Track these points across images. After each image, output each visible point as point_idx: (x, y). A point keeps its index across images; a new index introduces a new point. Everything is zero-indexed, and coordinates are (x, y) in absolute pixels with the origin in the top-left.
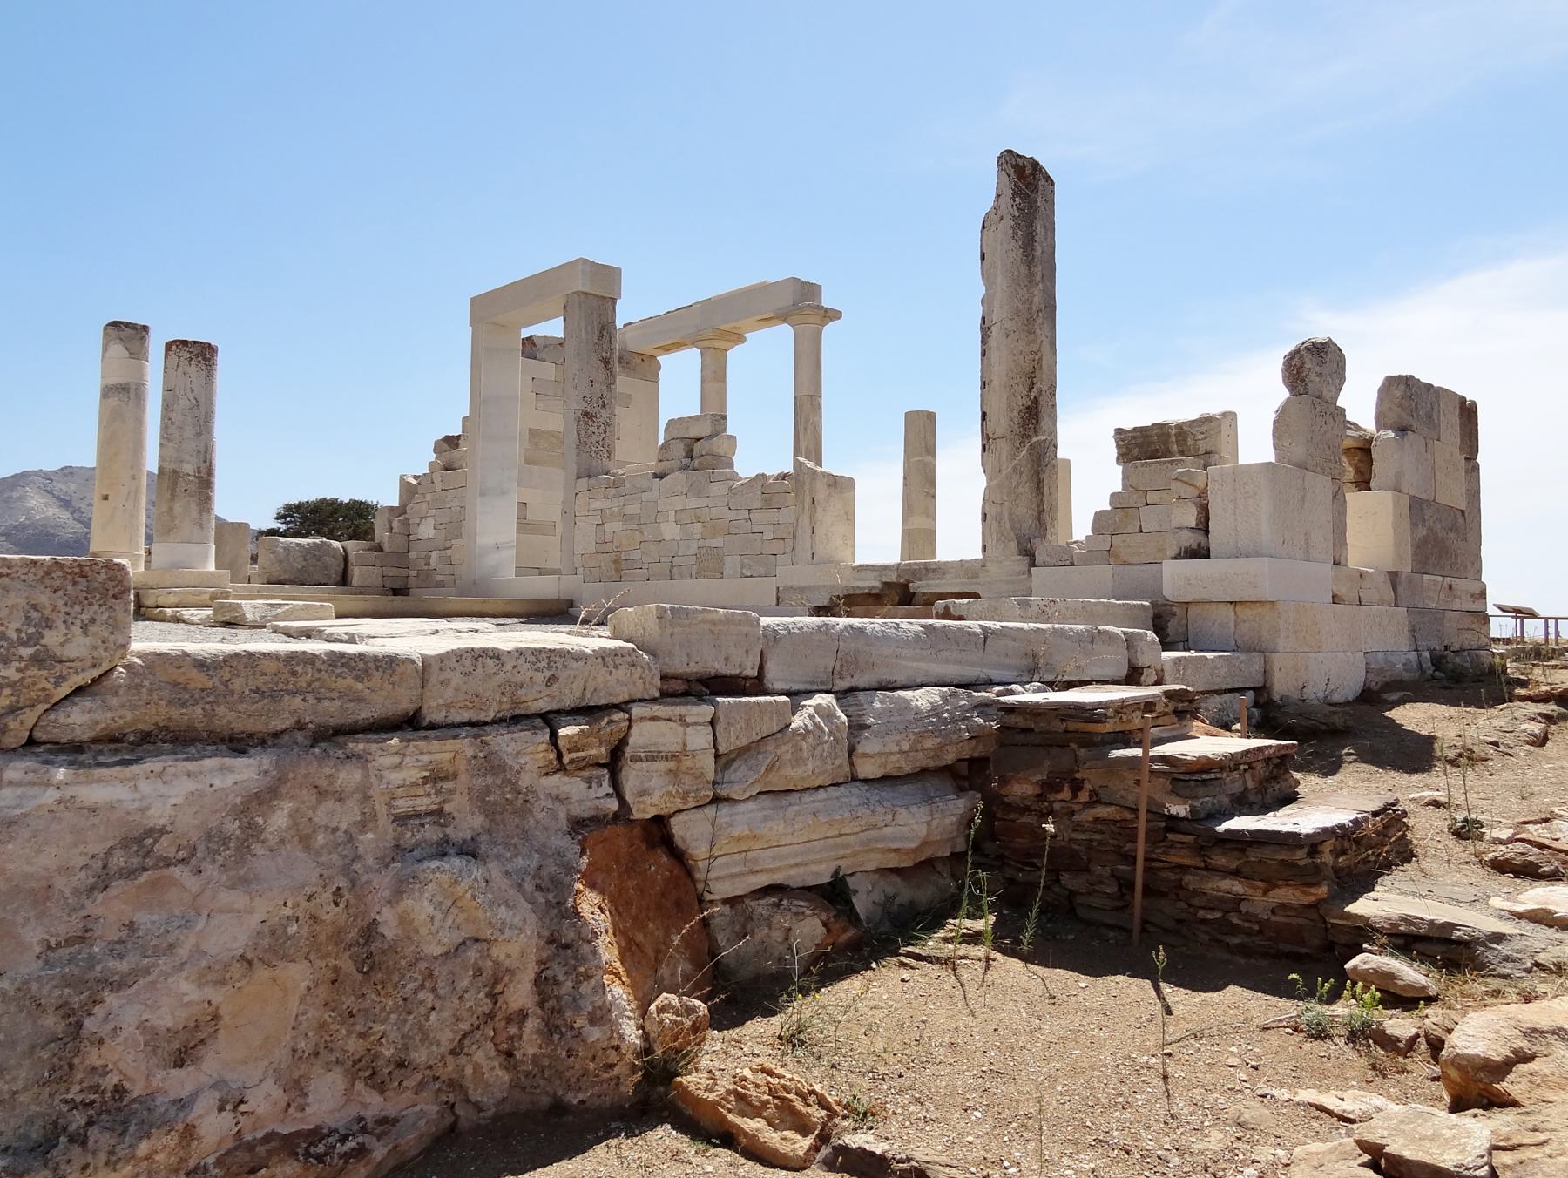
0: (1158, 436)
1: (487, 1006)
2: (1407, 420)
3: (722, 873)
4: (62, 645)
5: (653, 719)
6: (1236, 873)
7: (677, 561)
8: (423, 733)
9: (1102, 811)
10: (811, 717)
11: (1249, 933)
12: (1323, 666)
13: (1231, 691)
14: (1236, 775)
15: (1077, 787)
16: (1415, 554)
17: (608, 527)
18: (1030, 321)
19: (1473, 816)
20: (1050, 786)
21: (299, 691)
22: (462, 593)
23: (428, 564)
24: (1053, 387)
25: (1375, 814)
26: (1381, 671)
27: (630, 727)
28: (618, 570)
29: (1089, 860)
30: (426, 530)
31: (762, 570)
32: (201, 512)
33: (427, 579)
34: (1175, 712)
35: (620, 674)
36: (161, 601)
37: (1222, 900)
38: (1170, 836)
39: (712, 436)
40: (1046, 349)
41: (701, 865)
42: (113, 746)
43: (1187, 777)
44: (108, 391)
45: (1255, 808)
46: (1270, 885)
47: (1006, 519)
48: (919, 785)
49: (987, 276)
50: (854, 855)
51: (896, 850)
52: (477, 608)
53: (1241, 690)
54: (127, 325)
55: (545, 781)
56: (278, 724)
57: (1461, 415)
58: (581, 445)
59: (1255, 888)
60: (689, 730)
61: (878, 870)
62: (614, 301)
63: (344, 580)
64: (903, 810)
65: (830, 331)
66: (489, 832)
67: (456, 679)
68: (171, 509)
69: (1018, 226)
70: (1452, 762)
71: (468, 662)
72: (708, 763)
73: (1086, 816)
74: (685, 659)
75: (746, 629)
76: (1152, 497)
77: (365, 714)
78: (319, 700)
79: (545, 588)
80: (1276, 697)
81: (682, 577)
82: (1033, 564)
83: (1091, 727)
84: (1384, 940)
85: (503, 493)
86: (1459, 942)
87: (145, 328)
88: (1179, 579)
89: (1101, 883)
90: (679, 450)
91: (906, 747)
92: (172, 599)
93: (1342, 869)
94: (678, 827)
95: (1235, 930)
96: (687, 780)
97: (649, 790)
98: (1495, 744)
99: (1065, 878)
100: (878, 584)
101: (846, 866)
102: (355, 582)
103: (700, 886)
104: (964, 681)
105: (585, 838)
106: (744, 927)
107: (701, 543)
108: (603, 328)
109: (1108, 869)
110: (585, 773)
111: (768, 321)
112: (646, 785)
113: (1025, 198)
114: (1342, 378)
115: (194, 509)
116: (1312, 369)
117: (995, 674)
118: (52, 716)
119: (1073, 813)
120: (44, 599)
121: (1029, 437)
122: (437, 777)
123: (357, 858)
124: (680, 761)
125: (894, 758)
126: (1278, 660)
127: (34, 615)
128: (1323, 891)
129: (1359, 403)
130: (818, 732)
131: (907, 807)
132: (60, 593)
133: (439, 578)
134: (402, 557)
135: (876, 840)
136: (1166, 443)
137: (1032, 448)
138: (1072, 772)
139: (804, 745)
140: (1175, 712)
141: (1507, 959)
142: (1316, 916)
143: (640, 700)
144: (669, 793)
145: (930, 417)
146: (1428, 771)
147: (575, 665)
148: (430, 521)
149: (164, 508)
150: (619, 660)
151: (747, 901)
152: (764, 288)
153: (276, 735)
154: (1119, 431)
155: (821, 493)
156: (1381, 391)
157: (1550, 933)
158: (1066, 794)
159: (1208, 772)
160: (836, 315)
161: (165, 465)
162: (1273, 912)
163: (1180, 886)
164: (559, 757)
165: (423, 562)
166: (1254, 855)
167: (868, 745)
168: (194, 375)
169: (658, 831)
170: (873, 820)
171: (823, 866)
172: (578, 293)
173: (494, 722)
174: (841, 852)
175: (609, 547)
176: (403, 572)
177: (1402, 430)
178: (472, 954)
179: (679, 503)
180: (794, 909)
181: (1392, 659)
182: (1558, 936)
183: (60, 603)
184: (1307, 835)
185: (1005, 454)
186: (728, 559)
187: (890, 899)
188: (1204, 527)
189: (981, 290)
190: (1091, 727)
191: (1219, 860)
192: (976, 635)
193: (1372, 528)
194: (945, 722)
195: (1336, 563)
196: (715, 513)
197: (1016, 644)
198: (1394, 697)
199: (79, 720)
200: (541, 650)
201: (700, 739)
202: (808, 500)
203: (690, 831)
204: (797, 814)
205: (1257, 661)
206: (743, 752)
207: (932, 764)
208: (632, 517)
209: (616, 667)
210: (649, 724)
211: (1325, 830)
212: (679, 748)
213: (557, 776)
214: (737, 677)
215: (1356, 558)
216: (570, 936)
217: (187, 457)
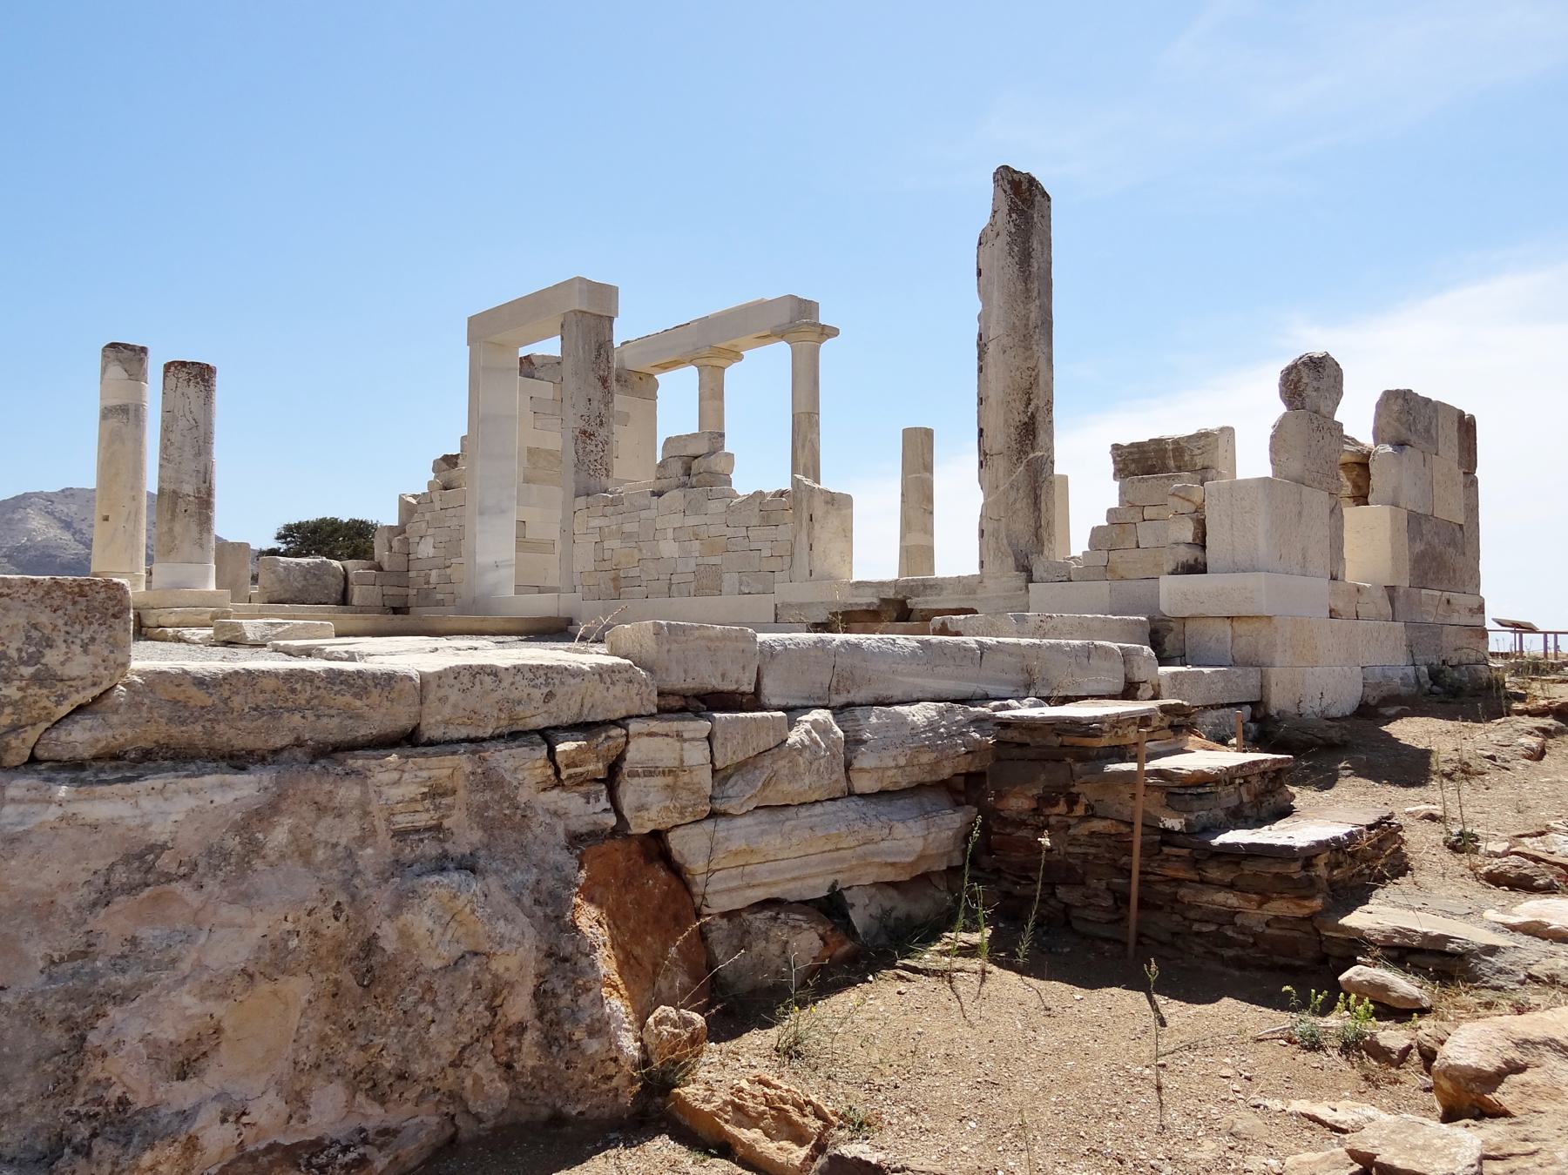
0: (1156, 451)
2: (1405, 434)
4: (63, 664)
5: (651, 734)
6: (1231, 887)
7: (675, 579)
8: (424, 750)
9: (1098, 825)
10: (808, 732)
11: (1243, 946)
12: (1320, 680)
13: (1229, 705)
14: (1231, 788)
15: (1072, 801)
16: (1413, 569)
17: (606, 544)
18: (1026, 338)
19: (1469, 830)
20: (1046, 800)
21: (299, 709)
22: (463, 611)
23: (428, 583)
24: (1050, 403)
25: (1370, 827)
26: (1379, 685)
27: (627, 743)
28: (617, 588)
29: (1085, 874)
30: (425, 549)
31: (760, 588)
32: (200, 533)
33: (426, 597)
34: (1171, 726)
35: (617, 690)
36: (162, 621)
37: (1217, 913)
38: (1166, 850)
39: (709, 454)
40: (1042, 365)
41: (698, 879)
42: (113, 764)
43: (1182, 791)
44: (107, 413)
45: (1250, 822)
46: (1265, 899)
47: (1003, 535)
48: (916, 799)
49: (983, 293)
50: (851, 869)
51: (893, 864)
52: (476, 626)
53: (1238, 705)
54: (126, 346)
55: (543, 797)
56: (278, 741)
57: (1459, 428)
58: (579, 463)
59: (1250, 901)
60: (686, 745)
61: (875, 884)
62: (611, 319)
63: (344, 599)
64: (900, 825)
65: (827, 349)
66: (488, 847)
67: (454, 695)
68: (171, 530)
69: (1014, 242)
70: (1449, 776)
71: (466, 679)
72: (705, 778)
73: (1081, 830)
74: (682, 675)
75: (742, 645)
76: (1148, 513)
77: (364, 731)
78: (318, 717)
79: (544, 606)
80: (1273, 712)
81: (680, 594)
82: (1030, 580)
83: (1087, 742)
84: (1378, 952)
85: (503, 512)
86: (1453, 954)
87: (144, 350)
88: (1175, 594)
89: (1097, 896)
90: (677, 467)
91: (902, 761)
92: (174, 619)
93: (1337, 882)
94: (675, 841)
95: (1229, 942)
96: (684, 794)
97: (646, 805)
98: (1492, 758)
99: (1061, 891)
100: (875, 600)
101: (843, 880)
102: (355, 601)
103: (698, 900)
104: (962, 696)
105: (583, 853)
106: (741, 941)
107: (700, 561)
108: (600, 347)
109: (1104, 883)
110: (583, 789)
111: (766, 338)
112: (644, 800)
113: (1021, 213)
114: (1340, 393)
115: (194, 529)
116: (1311, 383)
117: (992, 690)
118: (54, 735)
119: (1069, 827)
120: (44, 618)
121: (1026, 453)
123: (357, 873)
124: (677, 776)
125: (890, 773)
126: (1274, 674)
127: (35, 634)
128: (1317, 903)
129: (1357, 418)
130: (814, 747)
132: (60, 613)
133: (439, 597)
134: (402, 576)
135: (873, 854)
136: (1163, 458)
137: (1029, 464)
138: (1067, 786)
139: (801, 760)
140: (1171, 726)
141: (1500, 971)
142: (1309, 929)
143: (639, 716)
145: (928, 434)
146: (1425, 784)
147: (573, 682)
148: (430, 541)
149: (165, 528)
150: (616, 677)
151: (744, 915)
152: (761, 307)
153: (276, 751)
154: (1116, 447)
155: (819, 509)
156: (1378, 406)
157: (1544, 945)
158: (1062, 808)
159: (1203, 785)
160: (834, 332)
161: (165, 485)
162: (1268, 924)
163: (1175, 899)
164: (557, 772)
165: (422, 580)
166: (1249, 868)
167: (865, 760)
169: (656, 846)
171: (820, 880)
172: (575, 312)
173: (492, 738)
174: (838, 867)
175: (607, 565)
176: (402, 591)
177: (1400, 444)
178: (472, 967)
179: (677, 520)
180: (791, 923)
181: (1390, 673)
182: (1552, 948)
183: (60, 622)
184: (1302, 848)
185: (1001, 470)
186: (726, 577)
187: (887, 913)
188: (1201, 542)
189: (978, 306)
190: (1087, 742)
191: (1214, 873)
192: (973, 650)
193: (1370, 542)
194: (941, 737)
195: (1334, 578)
196: (713, 531)
198: (1392, 711)
199: (81, 738)
200: (539, 667)
201: (697, 754)
202: (806, 516)
203: (688, 845)
204: (794, 828)
205: (1253, 677)
206: (741, 766)
207: (928, 779)
208: (630, 535)
209: (613, 683)
210: (646, 739)
211: (1319, 843)
212: (677, 764)
213: (555, 792)
214: (733, 693)
215: (1353, 574)
216: (569, 949)
217: (186, 478)
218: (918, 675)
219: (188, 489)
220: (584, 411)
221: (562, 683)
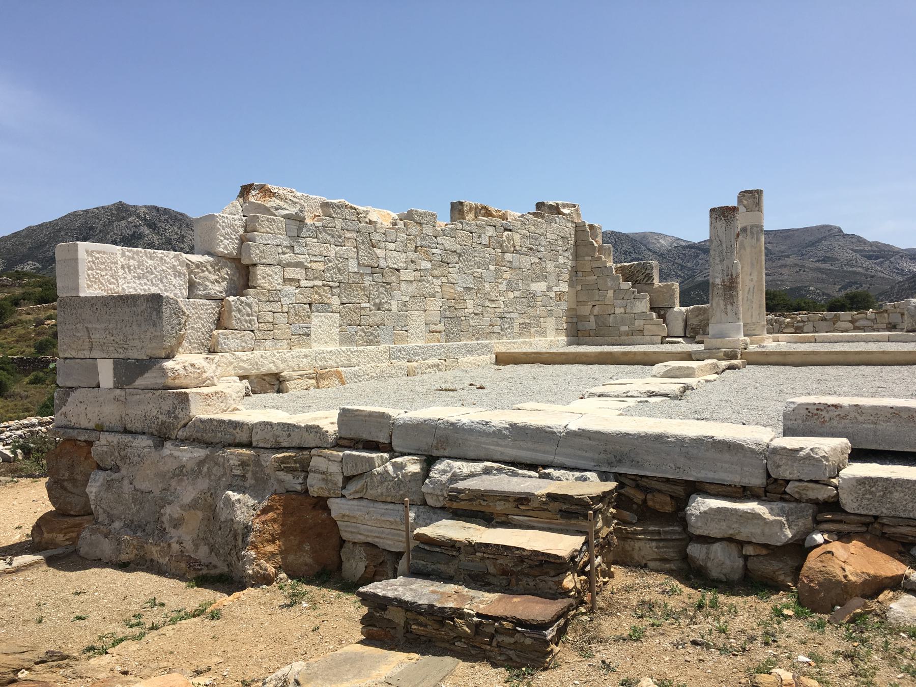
72: (340, 479)
75: (379, 420)
87: (759, 192)
97: (315, 486)
144: (322, 488)
203: (337, 507)
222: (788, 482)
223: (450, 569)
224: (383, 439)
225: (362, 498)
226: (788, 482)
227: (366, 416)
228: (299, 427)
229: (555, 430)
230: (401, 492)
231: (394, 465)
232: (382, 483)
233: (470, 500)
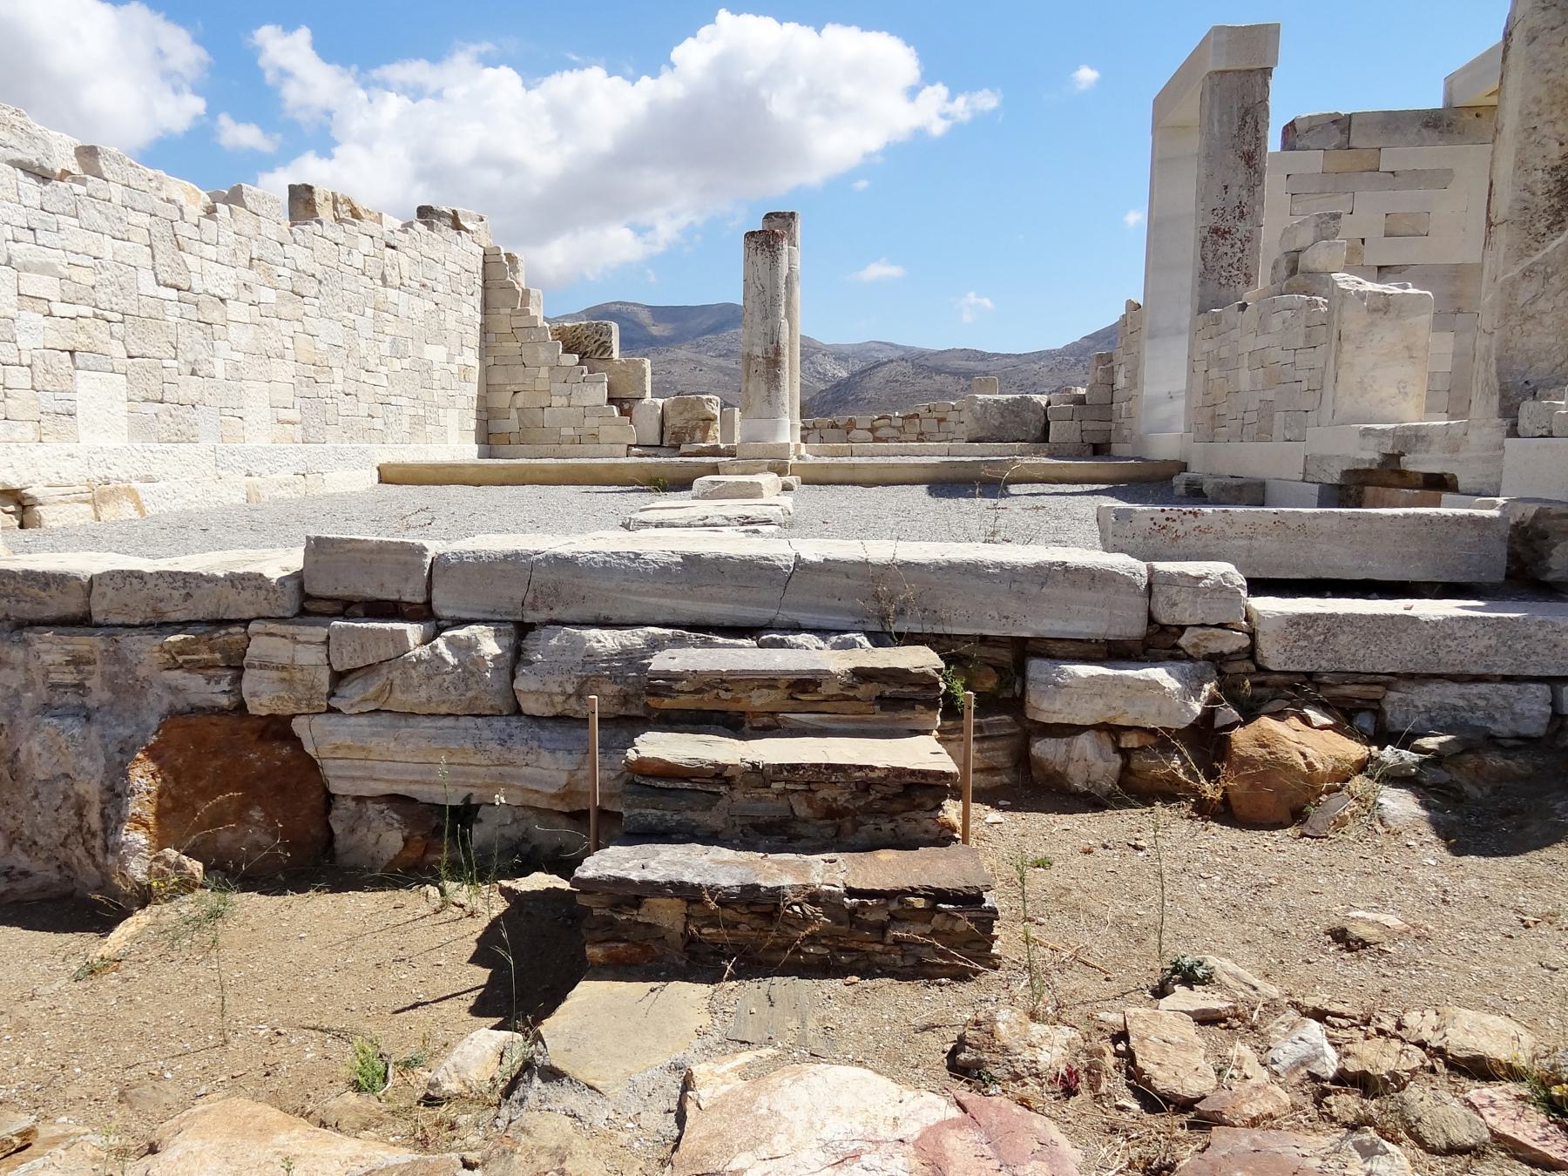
1: (75, 822)
3: (340, 773)
21: (7, 596)
60: (299, 647)
63: (1044, 436)
66: (112, 705)
67: (110, 593)
71: (118, 580)
72: (324, 677)
75: (402, 558)
82: (1513, 432)
94: (299, 726)
100: (1377, 456)
101: (477, 795)
110: (211, 672)
115: (763, 387)
122: (77, 661)
123: (19, 707)
131: (553, 751)
168: (760, 263)
169: (278, 729)
170: (509, 756)
173: (141, 625)
176: (1104, 425)
178: (61, 785)
180: (389, 820)
197: (853, 582)
200: (177, 573)
201: (310, 656)
202: (1335, 335)
203: (314, 734)
204: (411, 736)
213: (178, 672)
216: (119, 789)
217: (756, 341)
218: (665, 595)
219: (758, 351)
220: (1218, 204)
221: (198, 587)
222: (1182, 628)
223: (711, 819)
224: (412, 593)
225: (377, 711)
226: (1182, 628)
227: (372, 551)
228: (212, 579)
229: (778, 563)
230: (470, 694)
231: (450, 643)
232: (429, 678)
233: (698, 691)
